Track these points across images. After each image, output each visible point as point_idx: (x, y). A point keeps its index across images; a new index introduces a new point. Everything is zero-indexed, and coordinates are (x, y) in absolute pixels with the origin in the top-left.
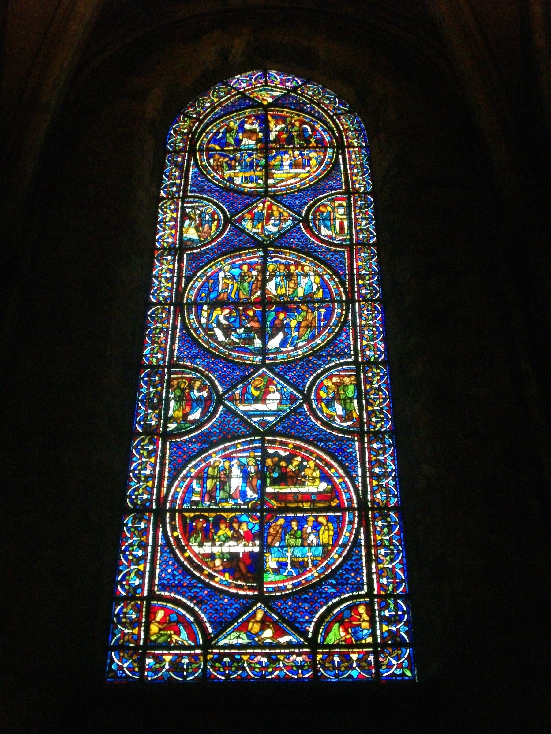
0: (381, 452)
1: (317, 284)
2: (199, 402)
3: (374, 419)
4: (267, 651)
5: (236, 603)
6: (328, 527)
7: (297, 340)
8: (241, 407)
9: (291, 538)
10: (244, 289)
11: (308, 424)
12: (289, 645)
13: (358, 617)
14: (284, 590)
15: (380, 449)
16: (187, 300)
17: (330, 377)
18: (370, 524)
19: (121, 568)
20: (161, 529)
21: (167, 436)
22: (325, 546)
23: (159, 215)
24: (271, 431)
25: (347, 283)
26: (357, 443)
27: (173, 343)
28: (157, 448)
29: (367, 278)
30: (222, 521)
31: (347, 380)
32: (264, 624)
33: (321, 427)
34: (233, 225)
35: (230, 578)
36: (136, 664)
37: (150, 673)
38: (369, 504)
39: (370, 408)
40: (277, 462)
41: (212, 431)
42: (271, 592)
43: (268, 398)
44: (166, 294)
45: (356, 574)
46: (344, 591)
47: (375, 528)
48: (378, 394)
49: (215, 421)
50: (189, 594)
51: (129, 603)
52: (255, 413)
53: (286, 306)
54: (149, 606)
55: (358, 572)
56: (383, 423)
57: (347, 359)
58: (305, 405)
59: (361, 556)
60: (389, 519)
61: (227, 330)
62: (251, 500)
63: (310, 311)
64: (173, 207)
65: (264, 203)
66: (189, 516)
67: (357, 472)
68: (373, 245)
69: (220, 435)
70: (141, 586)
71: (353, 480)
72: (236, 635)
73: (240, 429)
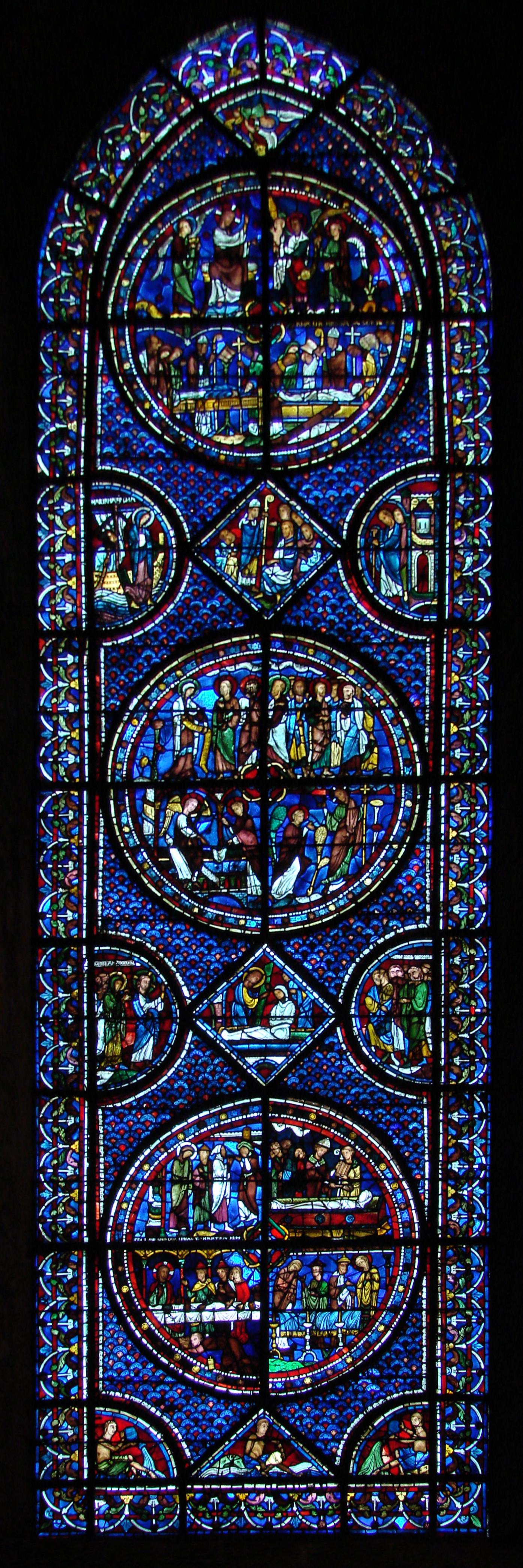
0: (465, 1129)
1: (368, 734)
2: (149, 1023)
3: (457, 1061)
4: (274, 1486)
5: (227, 1408)
6: (371, 1274)
7: (327, 878)
8: (226, 1035)
9: (310, 1295)
10: (225, 748)
11: (344, 1071)
12: (306, 1476)
13: (411, 1432)
14: (299, 1388)
15: (465, 1122)
16: (113, 775)
17: (384, 967)
18: (438, 1271)
19: (42, 1351)
20: (101, 1281)
21: (98, 1097)
22: (364, 1309)
23: (40, 534)
24: (279, 1087)
25: (427, 730)
26: (425, 1110)
27: (92, 886)
28: (82, 1121)
29: (467, 716)
30: (200, 1265)
31: (415, 972)
32: (271, 1443)
33: (365, 1076)
34: (198, 564)
35: (216, 1368)
36: (80, 1509)
37: (102, 1523)
38: (439, 1232)
39: (453, 1037)
40: (288, 1150)
41: (176, 1086)
42: (281, 1390)
43: (273, 1013)
44: (71, 759)
45: (410, 1360)
46: (391, 1388)
47: (445, 1279)
48: (469, 1006)
49: (180, 1065)
50: (153, 1394)
51: (62, 1411)
52: (251, 1046)
53: (307, 786)
54: (92, 1415)
55: (414, 1355)
56: (473, 1068)
57: (417, 923)
58: (338, 1029)
59: (421, 1328)
60: (468, 1261)
61: (196, 853)
62: (248, 1224)
63: (353, 804)
64: (67, 507)
65: (261, 497)
66: (145, 1255)
67: (423, 1169)
68: (484, 625)
69: (189, 1095)
70: (77, 1381)
71: (414, 1185)
72: (228, 1461)
73: (225, 1080)
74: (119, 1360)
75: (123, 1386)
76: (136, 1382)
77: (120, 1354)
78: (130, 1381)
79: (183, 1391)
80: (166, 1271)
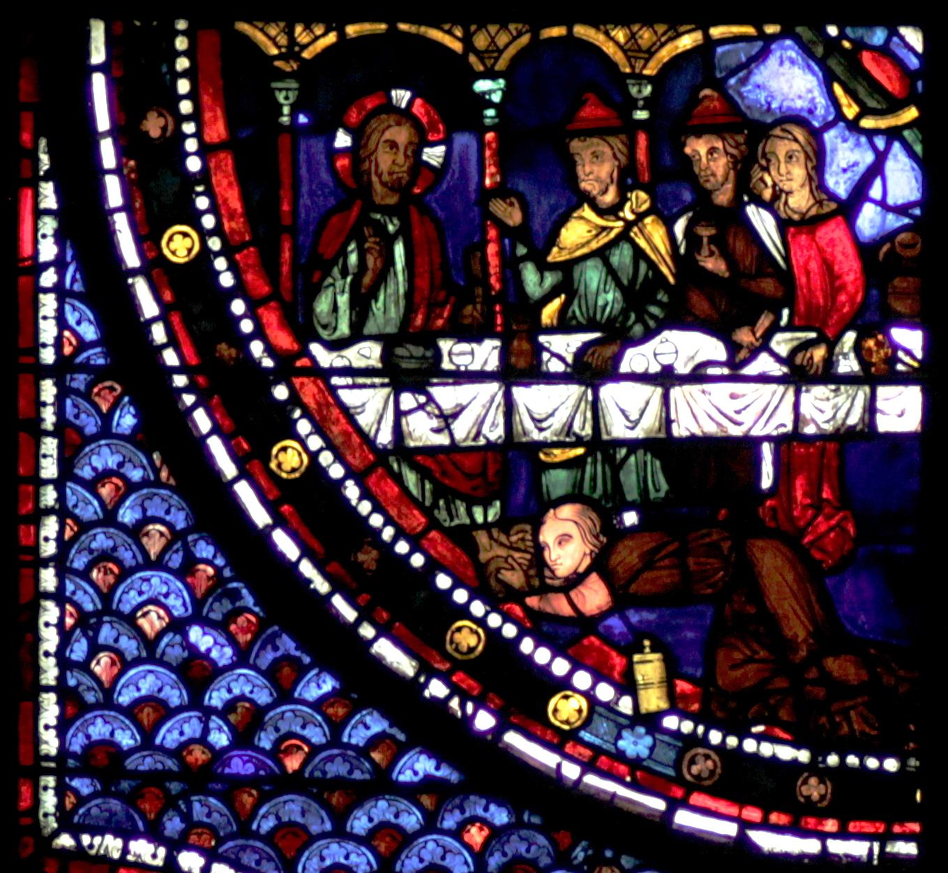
30: (591, 111)
35: (676, 705)
66: (292, 50)
74: (150, 650)
75: (170, 803)
76: (240, 782)
77: (152, 622)
78: (205, 776)
79: (497, 834)
80: (398, 142)
